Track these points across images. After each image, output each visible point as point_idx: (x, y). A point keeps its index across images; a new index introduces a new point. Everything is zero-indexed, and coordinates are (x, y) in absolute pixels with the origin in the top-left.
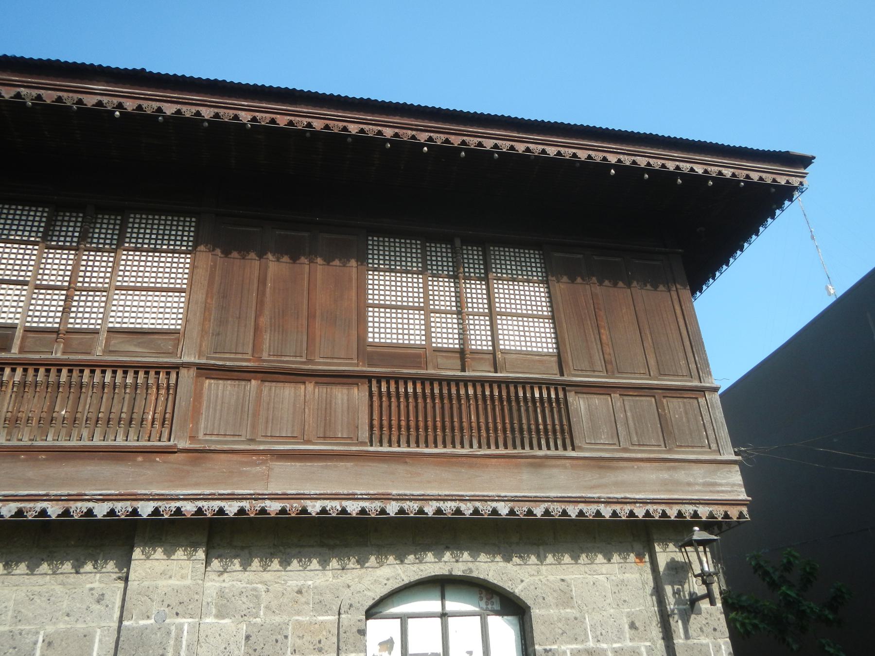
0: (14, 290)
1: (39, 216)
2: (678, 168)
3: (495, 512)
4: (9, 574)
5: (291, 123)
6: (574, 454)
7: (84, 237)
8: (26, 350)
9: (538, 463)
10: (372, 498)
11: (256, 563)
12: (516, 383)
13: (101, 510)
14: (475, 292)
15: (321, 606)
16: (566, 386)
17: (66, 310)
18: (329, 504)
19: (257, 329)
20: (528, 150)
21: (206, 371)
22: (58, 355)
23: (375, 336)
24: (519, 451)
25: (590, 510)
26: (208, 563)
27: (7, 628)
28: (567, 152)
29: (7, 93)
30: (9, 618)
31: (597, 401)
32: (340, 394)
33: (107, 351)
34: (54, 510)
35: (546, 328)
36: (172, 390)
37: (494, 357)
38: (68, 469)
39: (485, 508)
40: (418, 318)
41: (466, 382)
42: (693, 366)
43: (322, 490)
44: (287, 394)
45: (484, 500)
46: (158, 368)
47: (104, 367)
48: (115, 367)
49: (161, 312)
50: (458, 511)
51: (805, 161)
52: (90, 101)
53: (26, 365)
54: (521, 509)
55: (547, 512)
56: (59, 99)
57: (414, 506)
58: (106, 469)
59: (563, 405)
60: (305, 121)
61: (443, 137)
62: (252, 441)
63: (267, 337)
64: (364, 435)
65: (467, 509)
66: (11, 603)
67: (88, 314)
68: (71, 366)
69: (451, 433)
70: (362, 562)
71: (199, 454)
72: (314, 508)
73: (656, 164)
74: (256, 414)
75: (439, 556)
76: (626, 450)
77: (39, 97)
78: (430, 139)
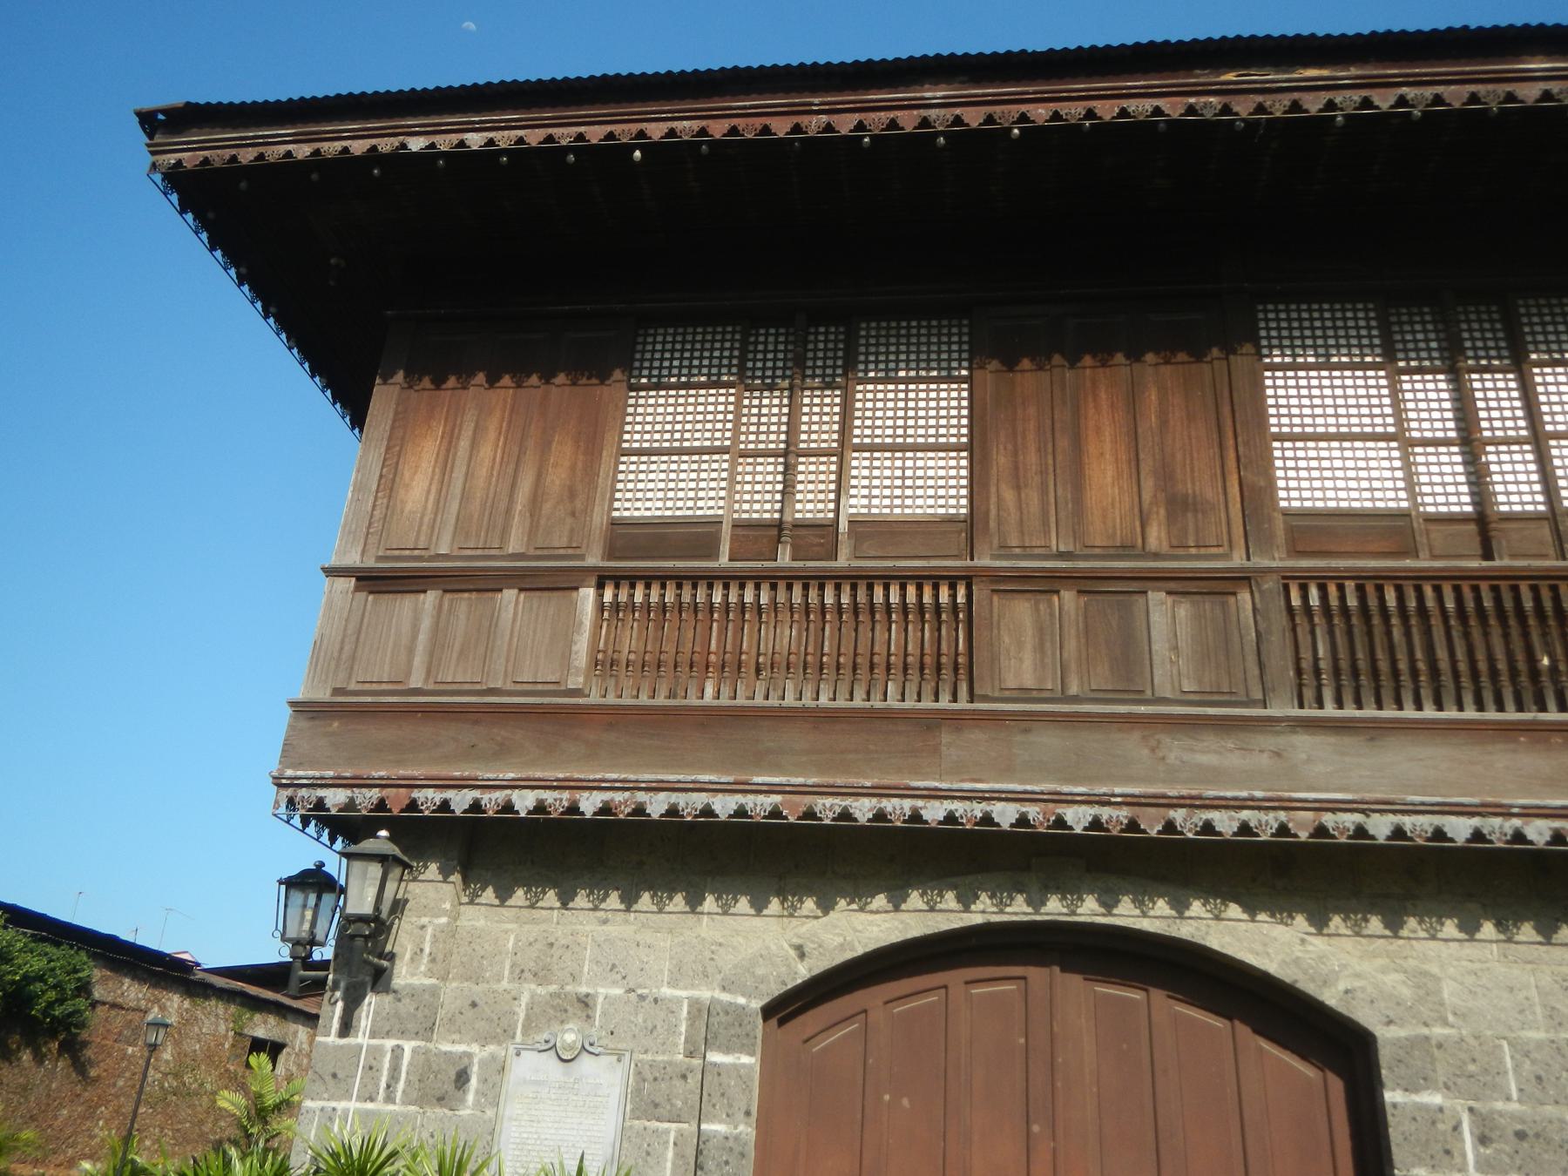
0: (1379, 450)
1: (1362, 317)
4: (1509, 940)
8: (1437, 552)
27: (1540, 1035)
29: (1385, 100)
30: (1540, 1017)
52: (1529, 93)
56: (1474, 98)
66: (1534, 993)
77: (1438, 100)
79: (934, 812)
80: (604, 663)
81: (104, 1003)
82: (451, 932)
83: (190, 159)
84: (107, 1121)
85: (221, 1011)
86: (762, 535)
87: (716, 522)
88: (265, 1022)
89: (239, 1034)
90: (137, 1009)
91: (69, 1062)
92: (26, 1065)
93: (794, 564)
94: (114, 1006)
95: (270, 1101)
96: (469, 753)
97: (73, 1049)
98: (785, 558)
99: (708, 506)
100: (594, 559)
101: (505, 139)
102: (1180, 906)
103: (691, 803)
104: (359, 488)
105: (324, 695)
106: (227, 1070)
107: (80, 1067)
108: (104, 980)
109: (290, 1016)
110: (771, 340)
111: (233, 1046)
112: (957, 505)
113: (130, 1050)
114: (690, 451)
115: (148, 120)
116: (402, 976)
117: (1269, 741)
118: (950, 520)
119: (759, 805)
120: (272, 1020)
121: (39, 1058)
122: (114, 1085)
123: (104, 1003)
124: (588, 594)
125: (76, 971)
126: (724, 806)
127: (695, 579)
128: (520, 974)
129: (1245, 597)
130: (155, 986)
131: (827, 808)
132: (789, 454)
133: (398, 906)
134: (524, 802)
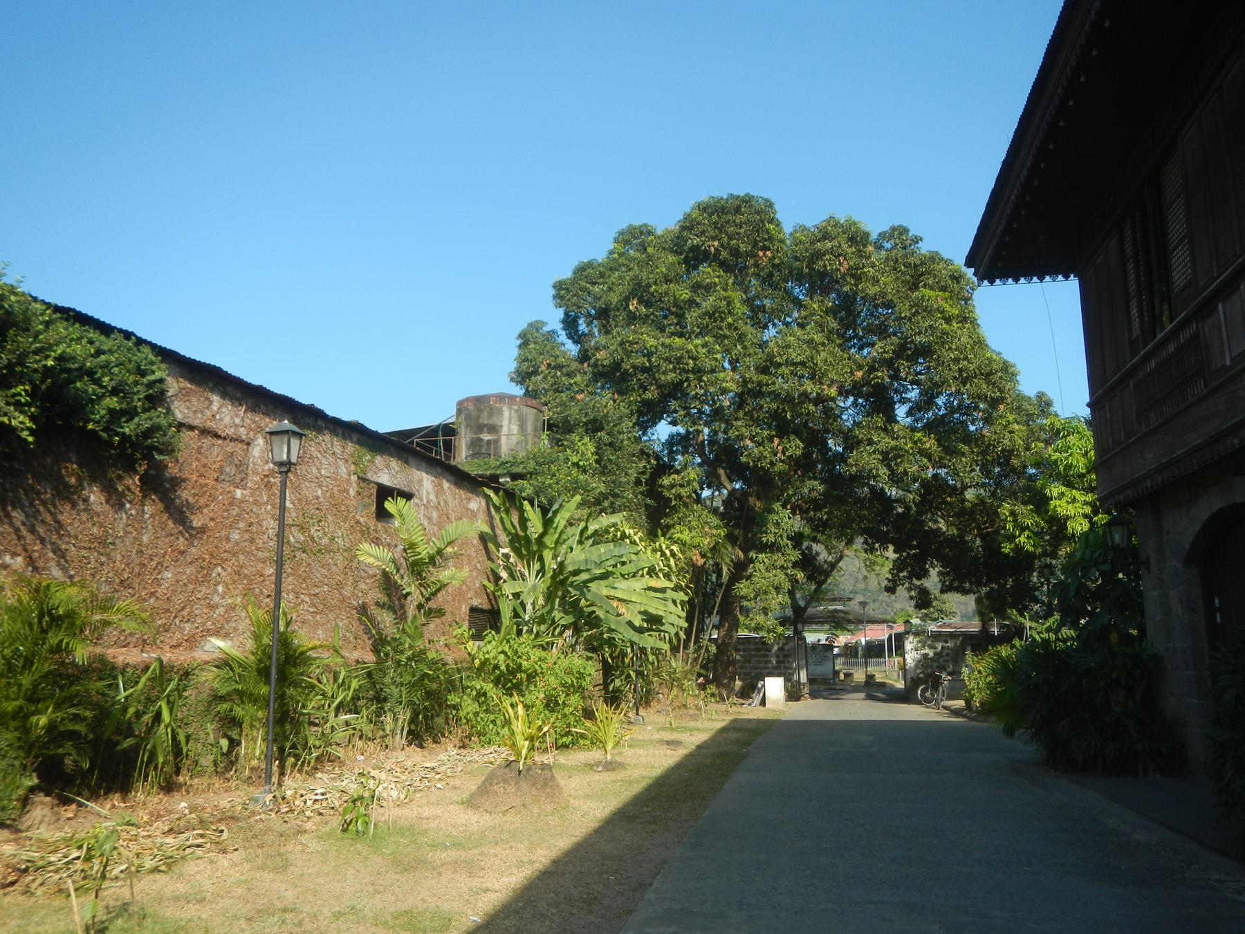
81: (191, 428)
84: (226, 585)
85: (338, 450)
88: (388, 467)
89: (362, 479)
90: (236, 440)
91: (160, 506)
92: (97, 508)
94: (205, 432)
95: (424, 551)
97: (160, 486)
106: (358, 522)
107: (178, 513)
108: (184, 394)
109: (412, 461)
111: (359, 494)
113: (239, 493)
120: (395, 464)
121: (116, 500)
122: (228, 539)
123: (191, 428)
125: (143, 374)
130: (253, 409)
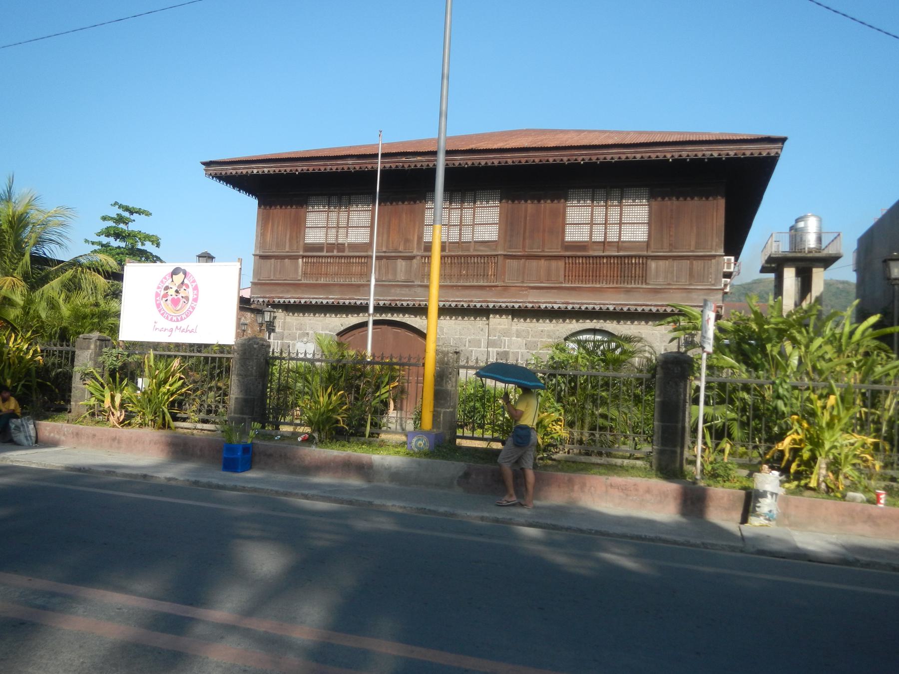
2: (704, 155)
3: (608, 309)
5: (527, 162)
6: (644, 286)
7: (463, 202)
9: (628, 291)
10: (563, 303)
11: (528, 320)
12: (625, 257)
13: (478, 305)
14: (614, 212)
15: (549, 336)
16: (647, 257)
17: (460, 234)
18: (548, 305)
19: (524, 239)
20: (627, 158)
21: (507, 257)
22: (460, 253)
23: (568, 238)
24: (622, 285)
25: (647, 309)
26: (513, 319)
28: (646, 155)
31: (661, 263)
32: (554, 264)
33: (475, 250)
34: (465, 305)
35: (645, 228)
36: (497, 263)
37: (619, 245)
38: (467, 292)
39: (604, 308)
40: (588, 227)
41: (603, 257)
42: (714, 244)
43: (546, 301)
44: (534, 263)
45: (604, 304)
46: (491, 256)
47: (474, 256)
48: (478, 256)
49: (490, 233)
50: (594, 308)
51: (783, 140)
52: (457, 163)
53: (451, 256)
54: (618, 309)
55: (629, 309)
57: (578, 306)
58: (479, 292)
59: (645, 268)
60: (532, 159)
61: (588, 157)
62: (523, 282)
63: (527, 241)
64: (562, 279)
65: (597, 308)
67: (467, 237)
68: (465, 256)
69: (596, 278)
70: (564, 321)
71: (506, 288)
72: (543, 306)
73: (692, 154)
74: (524, 273)
75: (591, 320)
76: (669, 284)
78: (583, 160)
79: (358, 302)
80: (305, 274)
82: (284, 322)
83: (213, 173)
86: (331, 247)
87: (323, 244)
93: (337, 253)
96: (282, 292)
98: (335, 253)
99: (322, 241)
100: (301, 253)
101: (272, 170)
102: (404, 315)
103: (319, 301)
104: (257, 236)
105: (256, 281)
110: (334, 199)
112: (367, 240)
114: (321, 225)
115: (204, 164)
116: (277, 330)
117: (413, 289)
118: (366, 243)
119: (330, 301)
124: (300, 260)
126: (325, 302)
127: (319, 257)
128: (297, 329)
129: (414, 261)
131: (341, 302)
132: (338, 227)
133: (275, 318)
134: (292, 301)
